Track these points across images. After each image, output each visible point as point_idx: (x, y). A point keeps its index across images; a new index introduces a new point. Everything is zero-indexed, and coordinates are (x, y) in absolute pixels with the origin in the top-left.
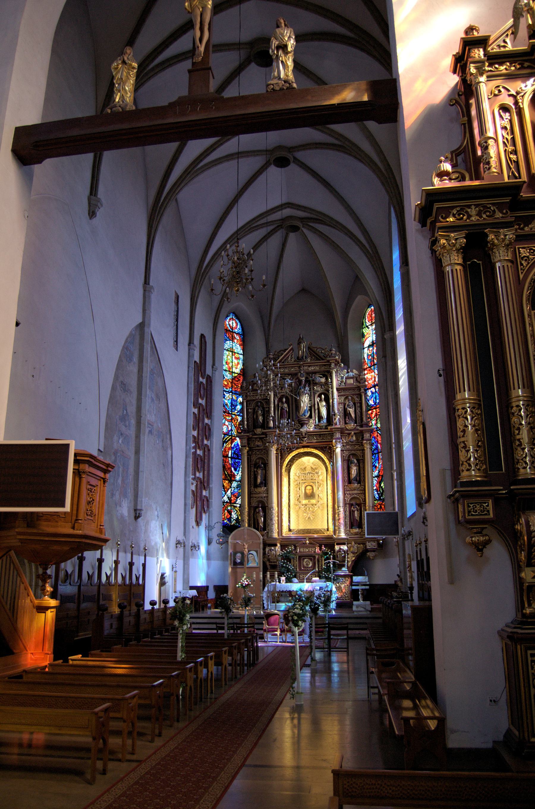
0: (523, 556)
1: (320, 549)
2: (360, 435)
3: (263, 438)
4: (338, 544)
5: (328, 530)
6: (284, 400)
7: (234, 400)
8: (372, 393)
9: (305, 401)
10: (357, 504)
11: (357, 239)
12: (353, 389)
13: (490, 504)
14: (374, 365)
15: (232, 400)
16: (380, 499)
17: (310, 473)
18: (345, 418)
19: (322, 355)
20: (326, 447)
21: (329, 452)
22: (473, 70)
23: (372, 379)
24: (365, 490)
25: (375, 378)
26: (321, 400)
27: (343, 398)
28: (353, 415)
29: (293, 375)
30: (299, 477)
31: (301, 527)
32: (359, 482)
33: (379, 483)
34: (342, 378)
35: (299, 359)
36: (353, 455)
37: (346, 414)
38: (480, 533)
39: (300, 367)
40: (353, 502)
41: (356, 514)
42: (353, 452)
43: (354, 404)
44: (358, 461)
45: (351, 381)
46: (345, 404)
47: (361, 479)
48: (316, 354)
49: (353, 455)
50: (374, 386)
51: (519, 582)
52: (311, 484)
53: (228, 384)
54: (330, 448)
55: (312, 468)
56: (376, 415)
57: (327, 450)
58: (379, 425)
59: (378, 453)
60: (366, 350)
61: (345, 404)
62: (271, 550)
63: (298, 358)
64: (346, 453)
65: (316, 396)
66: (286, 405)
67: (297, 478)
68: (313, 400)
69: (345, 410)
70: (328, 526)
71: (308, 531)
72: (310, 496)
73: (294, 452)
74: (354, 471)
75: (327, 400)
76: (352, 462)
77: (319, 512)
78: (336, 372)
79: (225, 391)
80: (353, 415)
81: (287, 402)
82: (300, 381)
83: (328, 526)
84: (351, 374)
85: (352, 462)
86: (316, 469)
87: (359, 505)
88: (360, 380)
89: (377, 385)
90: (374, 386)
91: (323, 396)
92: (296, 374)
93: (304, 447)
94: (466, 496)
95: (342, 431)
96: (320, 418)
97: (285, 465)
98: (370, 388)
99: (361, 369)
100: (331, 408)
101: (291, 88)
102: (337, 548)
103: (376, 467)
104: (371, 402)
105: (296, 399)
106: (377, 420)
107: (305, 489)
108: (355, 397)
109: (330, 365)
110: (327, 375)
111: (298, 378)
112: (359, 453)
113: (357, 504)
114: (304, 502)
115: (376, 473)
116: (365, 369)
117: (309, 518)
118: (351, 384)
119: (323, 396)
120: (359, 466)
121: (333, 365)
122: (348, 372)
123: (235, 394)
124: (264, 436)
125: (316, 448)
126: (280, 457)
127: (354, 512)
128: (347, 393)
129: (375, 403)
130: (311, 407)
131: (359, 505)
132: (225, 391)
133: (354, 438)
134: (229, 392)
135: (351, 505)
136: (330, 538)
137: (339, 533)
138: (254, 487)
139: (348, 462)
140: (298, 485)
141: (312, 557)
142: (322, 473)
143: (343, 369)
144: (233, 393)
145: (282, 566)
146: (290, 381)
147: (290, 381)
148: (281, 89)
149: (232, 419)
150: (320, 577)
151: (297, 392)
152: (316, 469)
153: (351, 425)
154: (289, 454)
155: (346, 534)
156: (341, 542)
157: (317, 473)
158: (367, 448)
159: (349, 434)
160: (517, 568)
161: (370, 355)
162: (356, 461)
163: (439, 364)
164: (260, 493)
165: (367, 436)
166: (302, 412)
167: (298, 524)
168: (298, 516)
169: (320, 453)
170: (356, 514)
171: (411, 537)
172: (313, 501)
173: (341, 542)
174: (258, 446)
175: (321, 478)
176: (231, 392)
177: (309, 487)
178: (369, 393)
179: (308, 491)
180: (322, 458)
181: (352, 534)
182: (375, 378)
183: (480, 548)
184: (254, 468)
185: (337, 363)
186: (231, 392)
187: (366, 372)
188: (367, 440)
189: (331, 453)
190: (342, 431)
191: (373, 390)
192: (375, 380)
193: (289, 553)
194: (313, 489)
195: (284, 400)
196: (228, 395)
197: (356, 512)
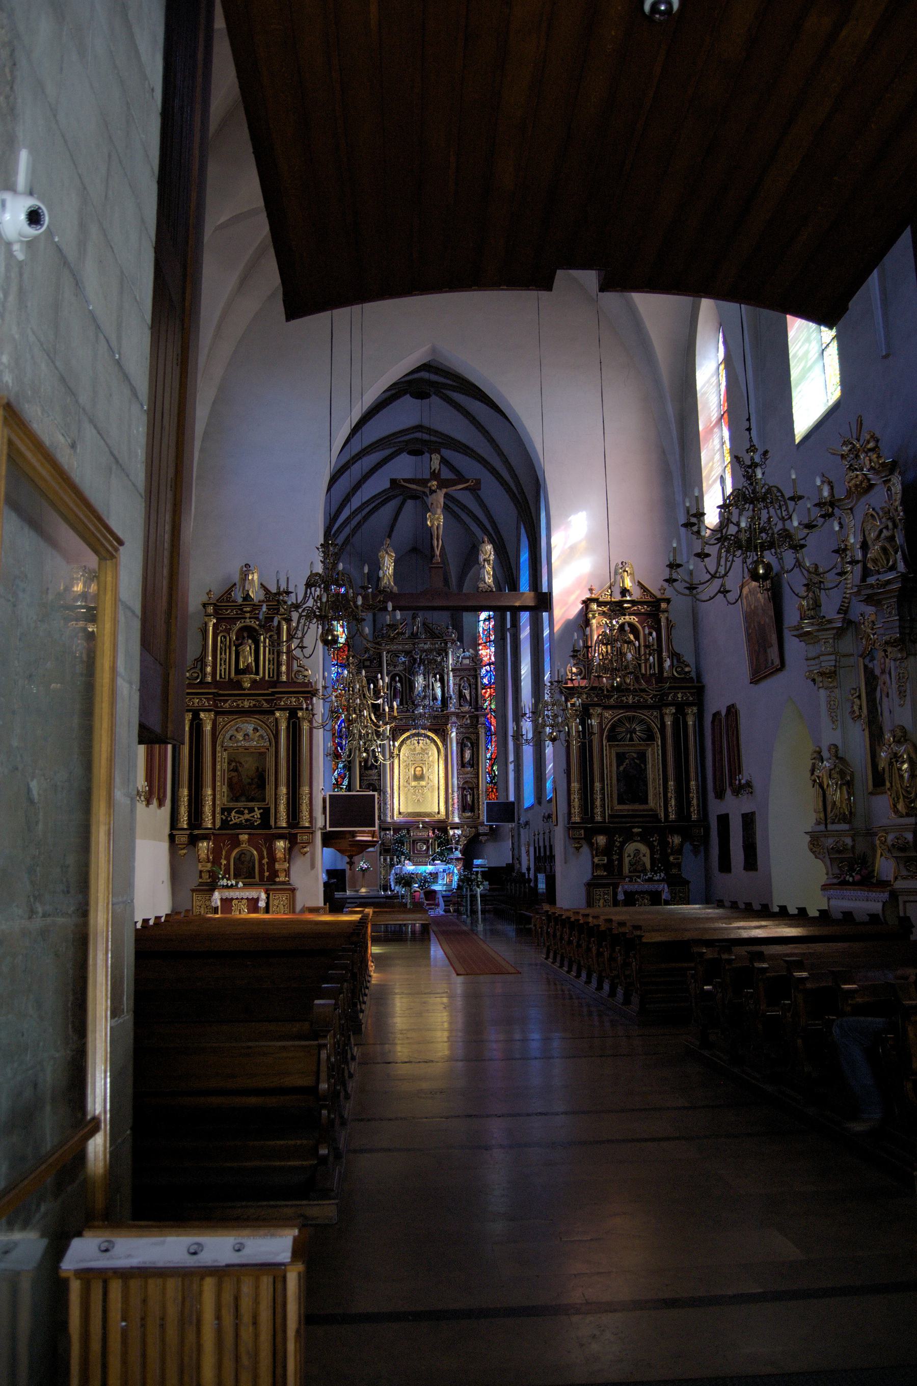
0: (594, 853)
1: (434, 833)
2: (475, 719)
4: (452, 828)
5: (439, 813)
6: (397, 678)
8: (487, 671)
9: (420, 682)
10: (470, 788)
11: (485, 528)
12: (469, 670)
13: (582, 832)
14: (490, 641)
16: (491, 782)
17: (419, 754)
18: (460, 700)
19: (437, 632)
21: (443, 734)
22: (591, 616)
23: (486, 655)
24: (478, 774)
25: (490, 655)
26: (436, 680)
27: (458, 679)
28: (468, 698)
29: (407, 653)
30: (408, 757)
31: (410, 810)
32: (472, 766)
33: (492, 766)
34: (458, 657)
35: (414, 636)
36: (467, 738)
37: (461, 696)
38: (578, 843)
39: (414, 644)
40: (466, 786)
41: (469, 798)
42: (467, 735)
43: (470, 685)
44: (472, 744)
45: (467, 661)
46: (460, 685)
47: (474, 763)
48: (431, 630)
49: (467, 738)
50: (489, 664)
51: (593, 862)
52: (421, 765)
54: (444, 731)
55: (422, 748)
56: (490, 695)
58: (493, 707)
59: (491, 735)
60: (481, 623)
61: (460, 685)
62: (386, 834)
63: (412, 634)
64: (461, 736)
65: (431, 675)
66: (399, 685)
67: (406, 759)
68: (427, 679)
69: (460, 692)
70: (439, 809)
71: (419, 814)
72: (419, 778)
74: (468, 755)
75: (442, 680)
76: (466, 746)
77: (429, 794)
78: (452, 652)
80: (468, 698)
81: (400, 681)
82: (415, 660)
83: (439, 809)
84: (467, 654)
85: (466, 746)
86: (426, 749)
87: (472, 789)
88: (477, 661)
89: (493, 663)
90: (489, 664)
91: (438, 676)
92: (411, 652)
94: (573, 828)
95: (457, 715)
96: (435, 698)
98: (485, 666)
99: (475, 645)
100: (446, 689)
101: (491, 591)
102: (451, 832)
103: (488, 749)
104: (485, 681)
105: (410, 679)
106: (491, 701)
107: (415, 771)
108: (470, 678)
109: (446, 644)
110: (444, 652)
111: (412, 656)
112: (473, 737)
113: (470, 788)
114: (414, 784)
115: (488, 755)
116: (480, 645)
117: (418, 800)
118: (467, 665)
119: (438, 676)
120: (473, 750)
121: (449, 645)
122: (464, 652)
123: (341, 666)
127: (466, 796)
128: (463, 673)
129: (490, 682)
130: (425, 687)
131: (472, 789)
133: (469, 722)
134: (334, 665)
135: (464, 789)
136: (440, 821)
137: (453, 817)
139: (462, 746)
140: (407, 766)
141: (426, 842)
142: (432, 755)
143: (459, 648)
145: (397, 850)
146: (403, 659)
147: (403, 659)
148: (486, 591)
150: (442, 861)
151: (411, 671)
152: (426, 749)
153: (466, 708)
154: (401, 735)
155: (460, 818)
156: (455, 827)
157: (427, 754)
158: (482, 732)
159: (464, 717)
160: (593, 858)
161: (486, 630)
162: (469, 745)
163: (565, 766)
164: (371, 775)
165: (482, 720)
166: (416, 693)
167: (407, 807)
168: (407, 798)
170: (469, 798)
171: (528, 827)
172: (423, 783)
173: (455, 827)
175: (431, 759)
176: (337, 665)
177: (418, 769)
178: (483, 671)
179: (417, 773)
180: (434, 740)
181: (464, 818)
182: (490, 655)
183: (578, 849)
185: (453, 642)
186: (337, 665)
187: (480, 648)
188: (482, 724)
189: (444, 736)
190: (457, 715)
191: (488, 668)
192: (490, 658)
193: (402, 837)
194: (423, 770)
195: (397, 678)
197: (468, 796)
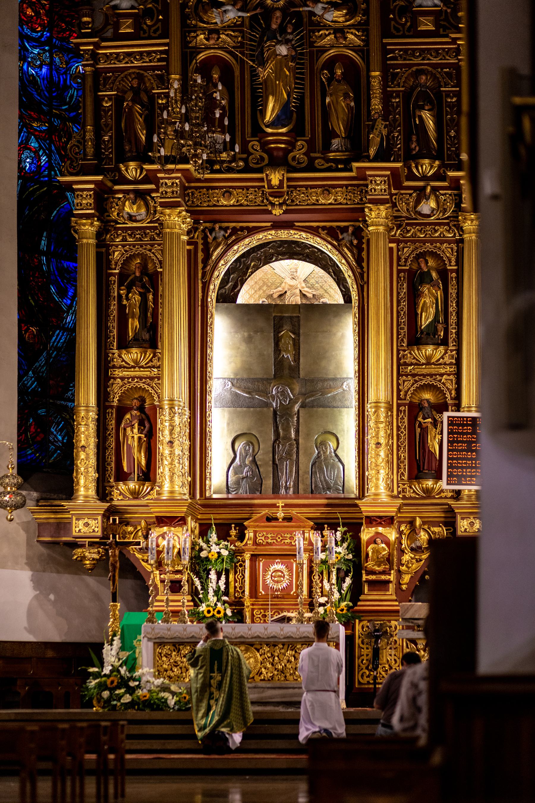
3: (149, 192)
7: (58, 69)
15: (50, 70)
20: (344, 230)
53: (37, 13)
57: (346, 237)
73: (247, 241)
79: (30, 39)
93: (278, 225)
97: (218, 282)
124: (153, 186)
125: (314, 231)
126: (200, 255)
132: (30, 39)
138: (119, 348)
144: (52, 47)
149: (52, 129)
169: (326, 248)
174: (131, 218)
176: (49, 41)
184: (120, 284)
196: (36, 51)
